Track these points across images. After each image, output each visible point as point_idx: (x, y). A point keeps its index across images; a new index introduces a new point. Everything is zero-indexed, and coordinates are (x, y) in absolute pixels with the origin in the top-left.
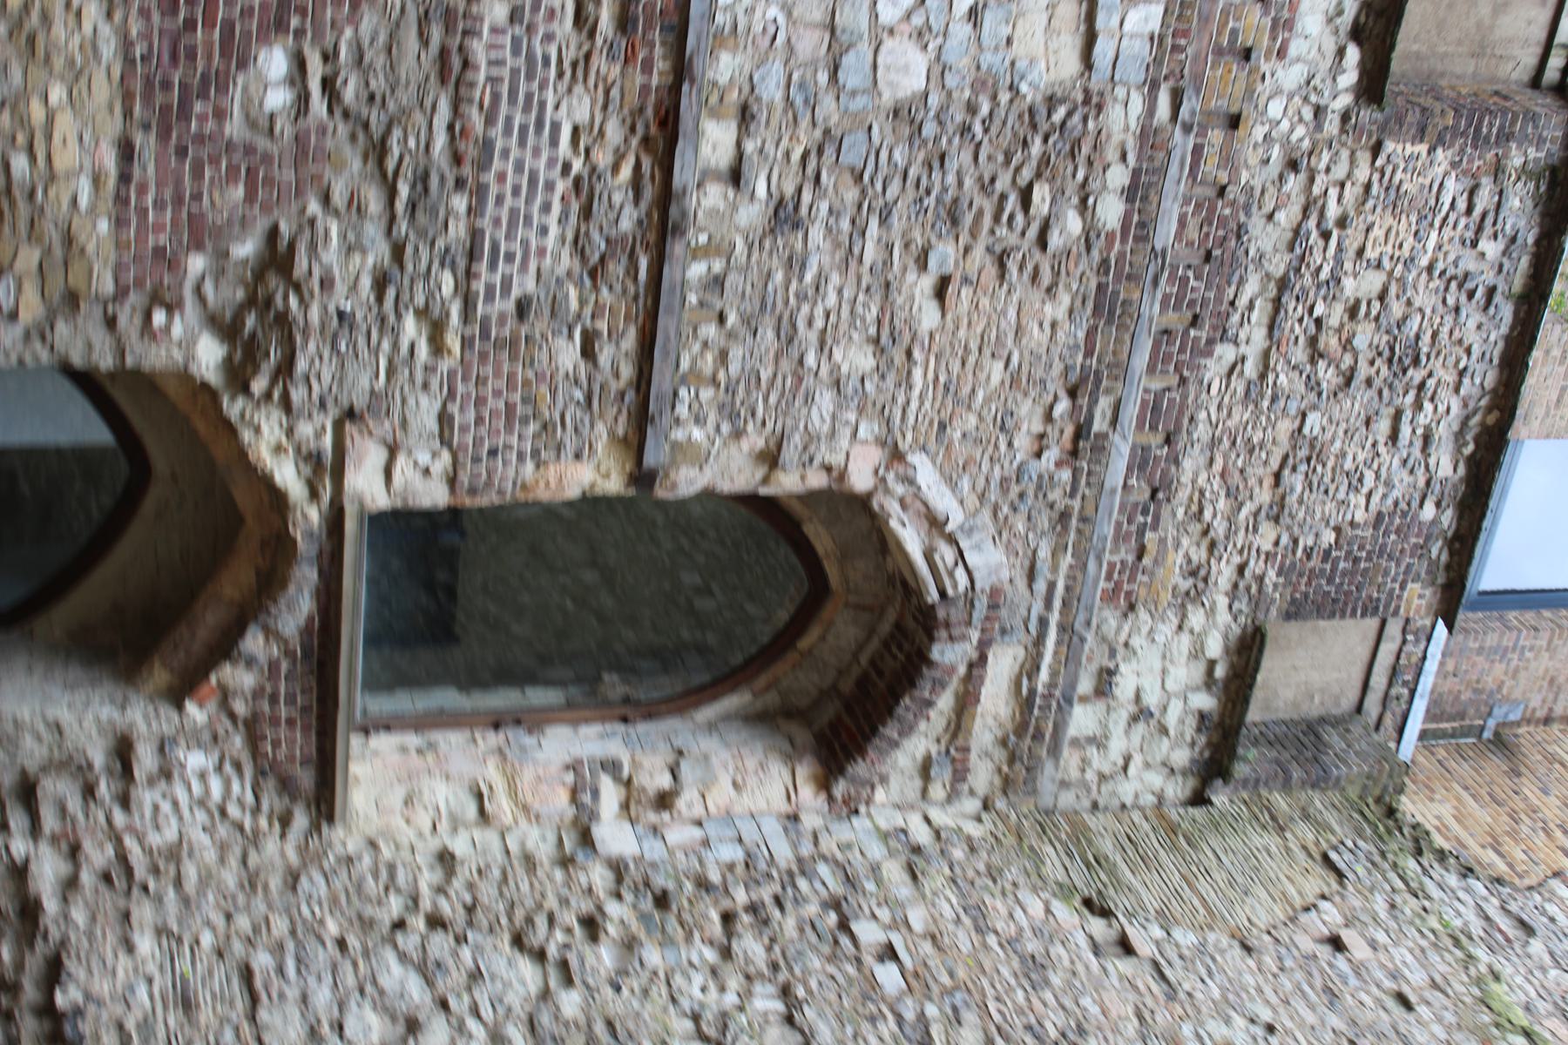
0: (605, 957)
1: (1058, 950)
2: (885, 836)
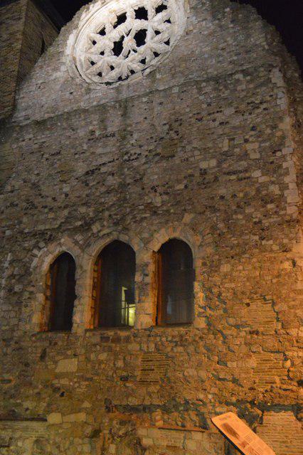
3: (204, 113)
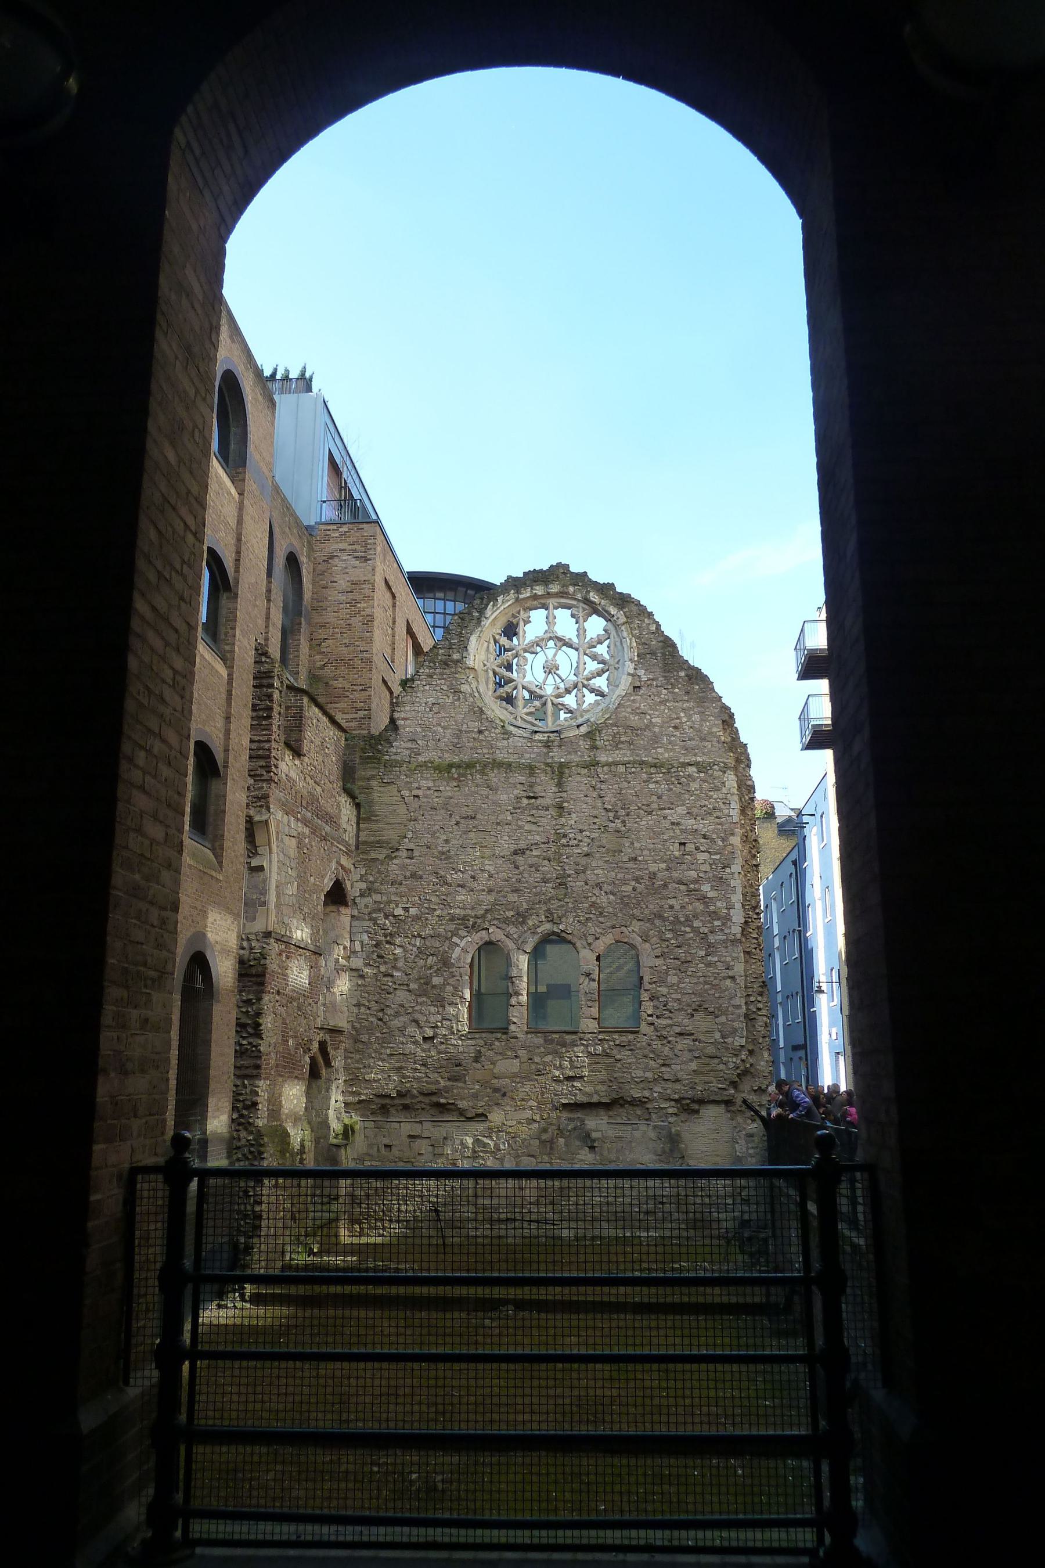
0: (396, 974)
2: (362, 895)
3: (654, 806)
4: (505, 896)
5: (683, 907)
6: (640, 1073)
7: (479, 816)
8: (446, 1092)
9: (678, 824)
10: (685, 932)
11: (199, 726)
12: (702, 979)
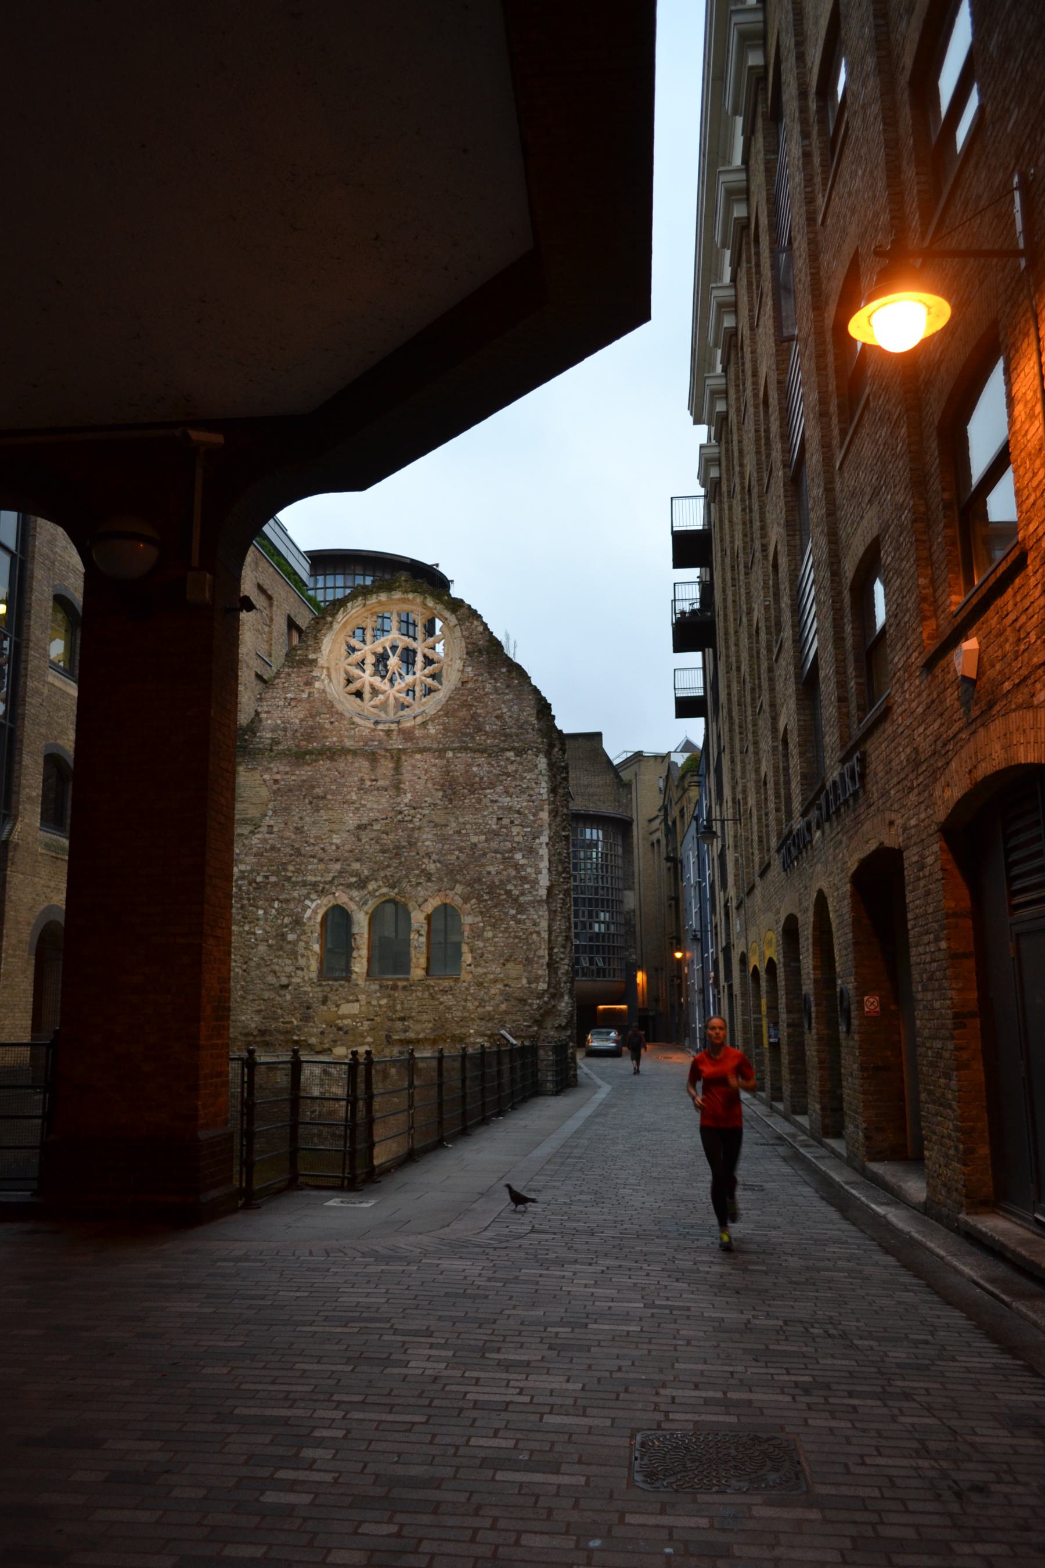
1: (270, 841)
4: (349, 865)
5: (498, 873)
6: (459, 1014)
7: (329, 797)
8: (299, 1030)
9: (496, 801)
10: (500, 894)
11: (52, 741)
12: (512, 934)
